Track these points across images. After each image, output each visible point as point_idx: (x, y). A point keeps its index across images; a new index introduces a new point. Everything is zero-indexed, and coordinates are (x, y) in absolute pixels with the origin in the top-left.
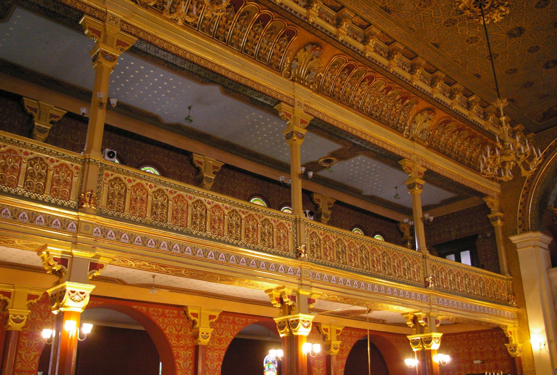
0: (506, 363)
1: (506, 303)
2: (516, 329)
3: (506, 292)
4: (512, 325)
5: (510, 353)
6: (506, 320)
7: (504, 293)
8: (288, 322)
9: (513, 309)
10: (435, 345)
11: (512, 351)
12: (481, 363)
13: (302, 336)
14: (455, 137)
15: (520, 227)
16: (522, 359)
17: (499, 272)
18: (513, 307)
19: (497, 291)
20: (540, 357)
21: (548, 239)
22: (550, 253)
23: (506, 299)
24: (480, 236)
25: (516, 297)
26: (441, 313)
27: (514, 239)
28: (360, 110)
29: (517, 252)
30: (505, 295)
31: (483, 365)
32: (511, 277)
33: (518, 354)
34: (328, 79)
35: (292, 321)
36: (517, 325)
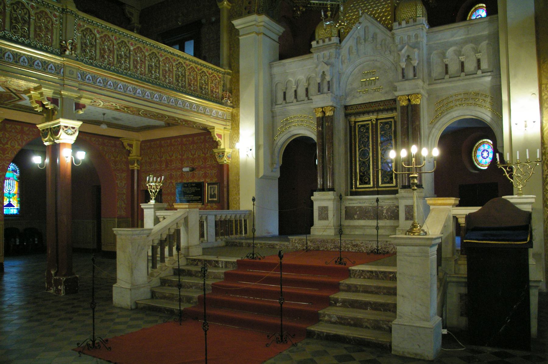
0: (214, 171)
1: (219, 101)
2: (228, 132)
3: (221, 88)
4: (222, 127)
5: (218, 160)
6: (213, 120)
7: (217, 88)
9: (225, 109)
10: (67, 139)
11: (219, 156)
12: (191, 171)
15: (245, 9)
16: (230, 165)
17: (218, 64)
18: (227, 105)
19: (207, 84)
20: (246, 164)
21: (279, 29)
22: (280, 46)
23: (220, 96)
24: (204, 21)
25: (230, 95)
26: (85, 94)
27: (238, 23)
29: (239, 39)
30: (220, 91)
31: (194, 173)
32: (229, 71)
33: (226, 160)
36: (230, 127)
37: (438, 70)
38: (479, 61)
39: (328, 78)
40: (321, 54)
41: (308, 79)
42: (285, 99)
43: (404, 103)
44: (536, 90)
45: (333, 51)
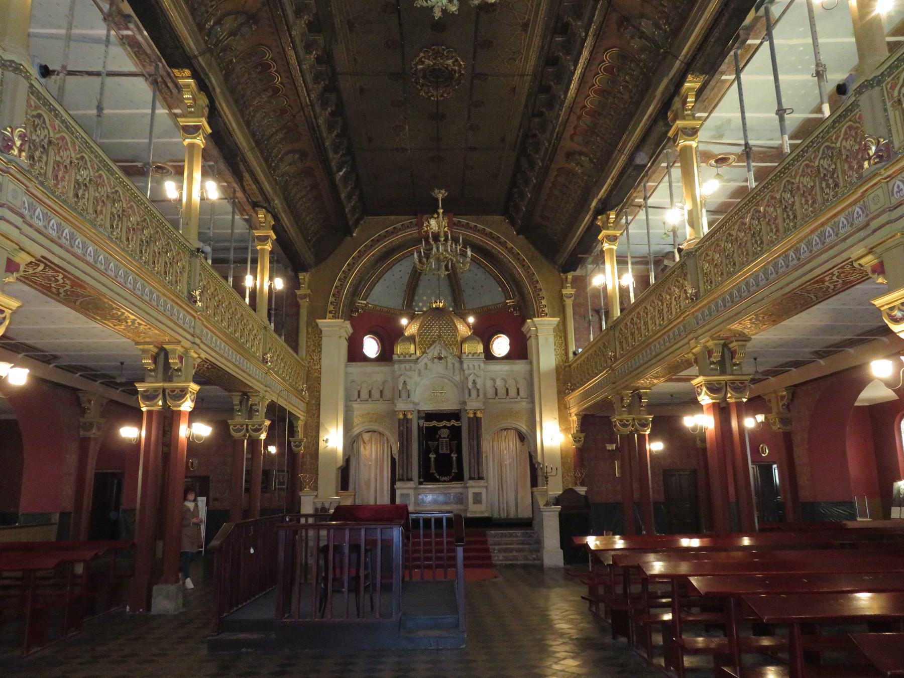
8: (164, 390)
13: (184, 412)
14: (304, 193)
28: (248, 123)
34: (238, 69)
35: (173, 391)
37: (490, 392)
38: (518, 389)
39: (408, 387)
40: (402, 366)
41: (384, 382)
42: (359, 396)
43: (472, 416)
44: (557, 416)
45: (412, 365)
